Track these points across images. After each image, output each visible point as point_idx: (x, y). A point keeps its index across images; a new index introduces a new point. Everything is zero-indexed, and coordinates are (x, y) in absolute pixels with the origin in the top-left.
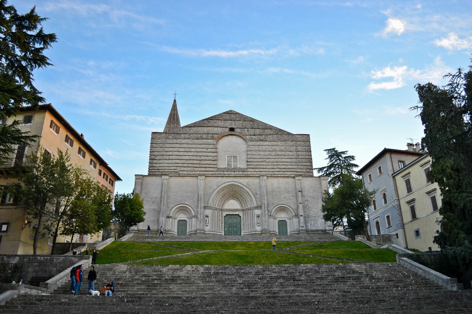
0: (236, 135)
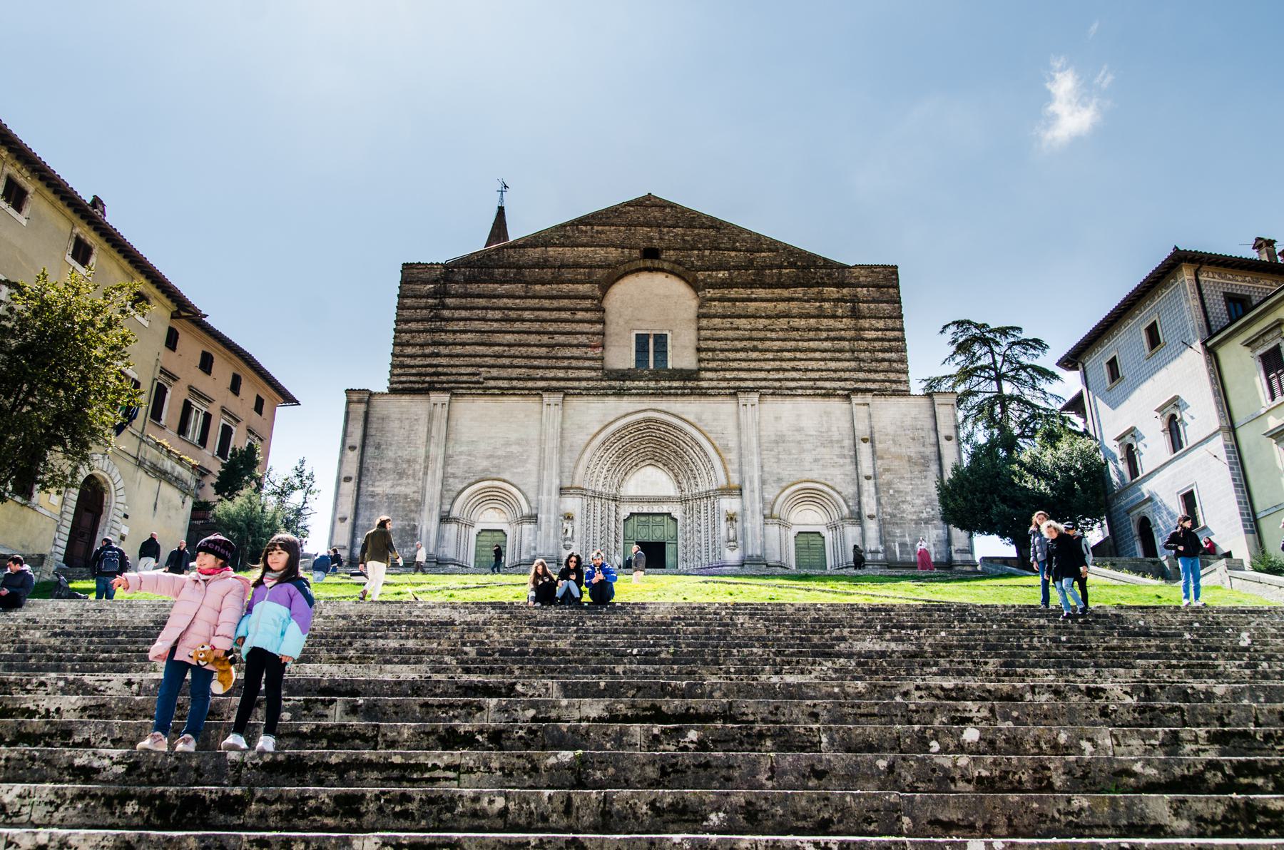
0: (662, 270)
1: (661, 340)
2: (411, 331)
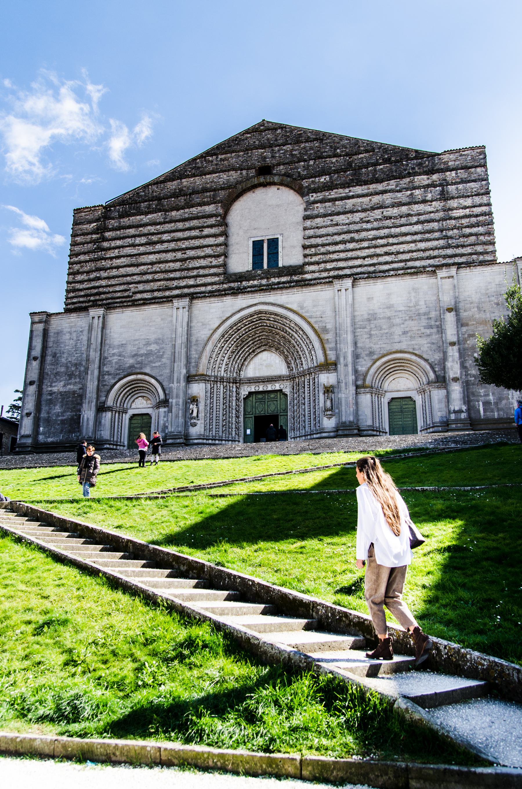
0: (273, 184)
1: (273, 243)
2: (80, 262)
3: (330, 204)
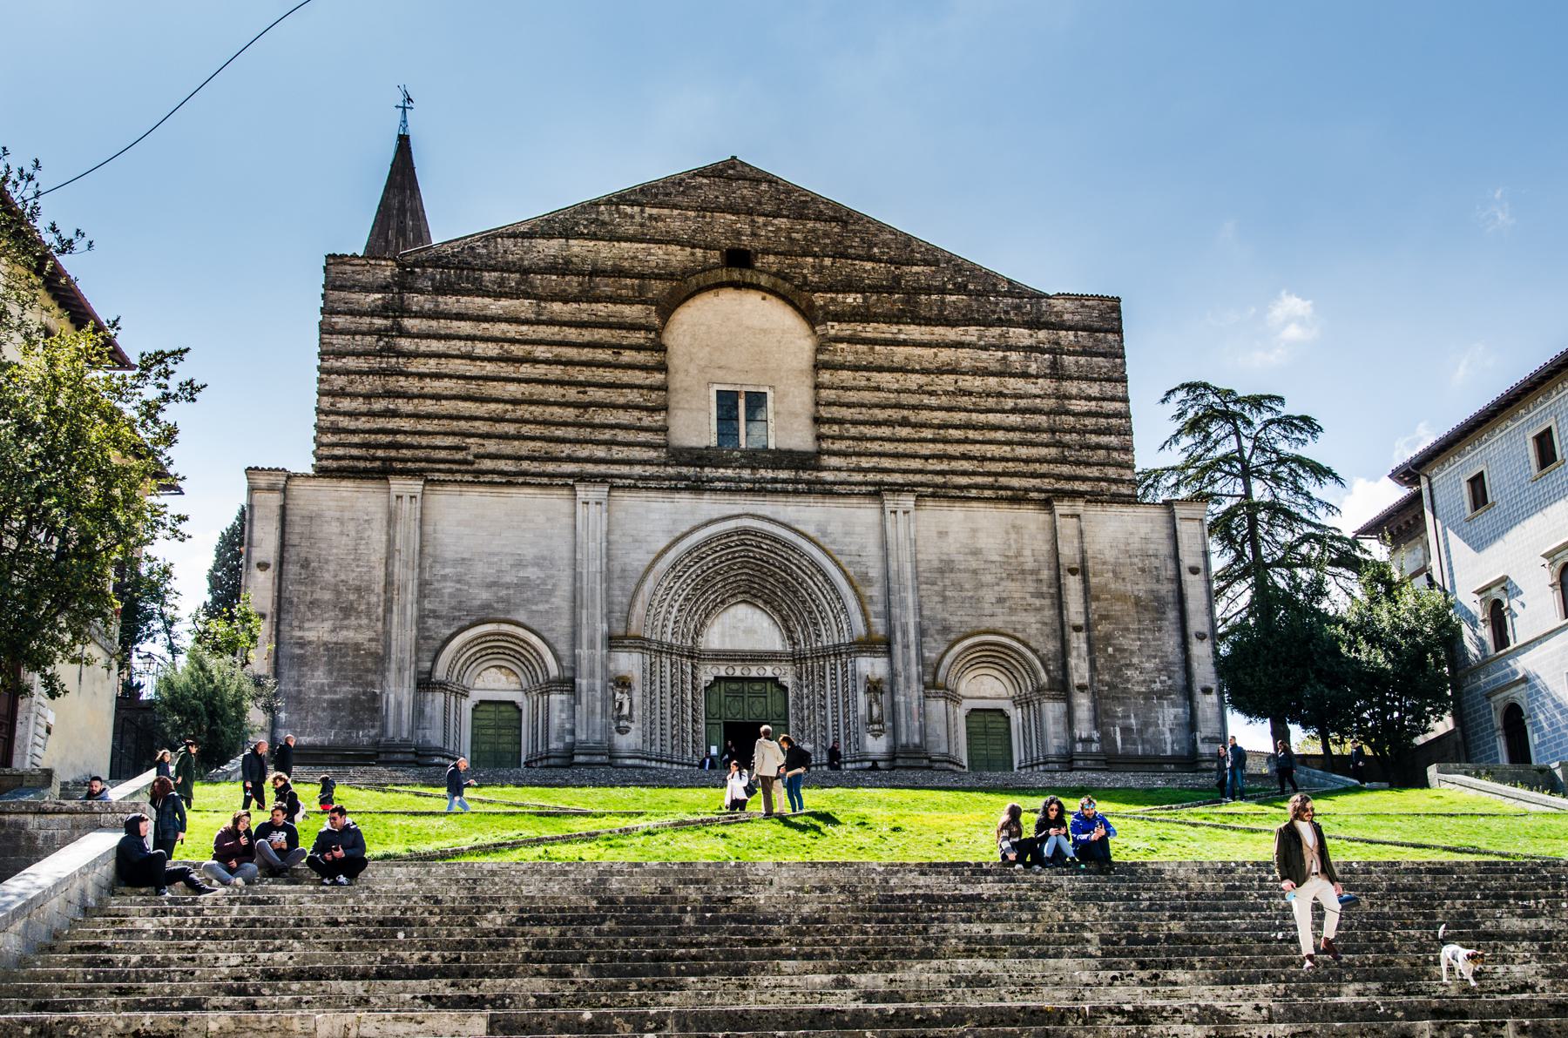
0: (757, 287)
2: (348, 372)
3: (864, 348)
